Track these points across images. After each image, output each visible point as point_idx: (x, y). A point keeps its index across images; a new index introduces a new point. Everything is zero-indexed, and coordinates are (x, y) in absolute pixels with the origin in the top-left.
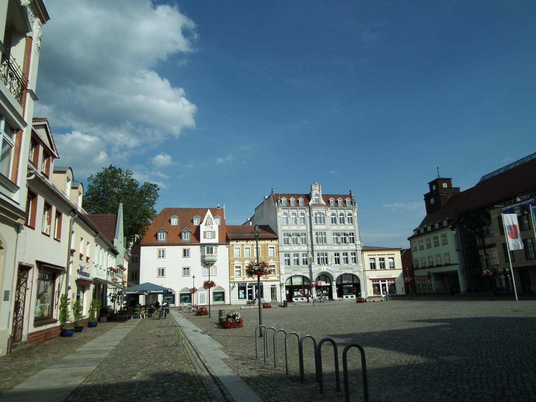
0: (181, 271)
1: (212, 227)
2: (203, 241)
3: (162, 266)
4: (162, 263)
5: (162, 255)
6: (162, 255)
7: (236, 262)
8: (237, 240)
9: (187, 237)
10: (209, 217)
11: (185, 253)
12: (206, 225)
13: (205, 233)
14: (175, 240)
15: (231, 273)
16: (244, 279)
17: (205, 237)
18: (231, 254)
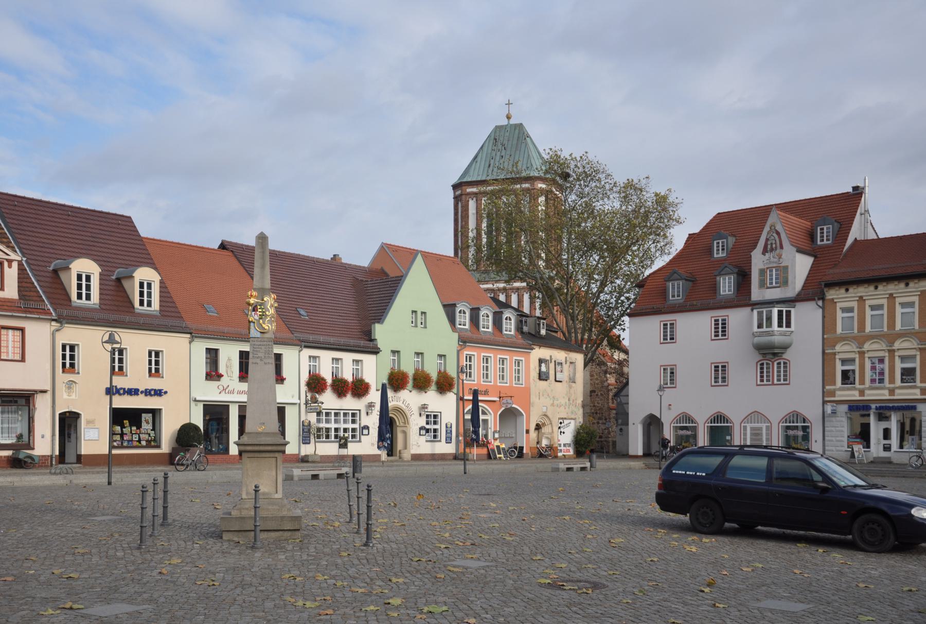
0: (708, 373)
1: (780, 257)
2: (756, 294)
3: (720, 359)
4: (669, 354)
5: (669, 335)
6: (669, 335)
7: (838, 348)
8: (846, 284)
9: (726, 286)
10: (773, 229)
11: (721, 330)
12: (765, 251)
13: (762, 272)
14: (701, 297)
15: (827, 377)
16: (862, 393)
17: (762, 284)
18: (828, 325)
